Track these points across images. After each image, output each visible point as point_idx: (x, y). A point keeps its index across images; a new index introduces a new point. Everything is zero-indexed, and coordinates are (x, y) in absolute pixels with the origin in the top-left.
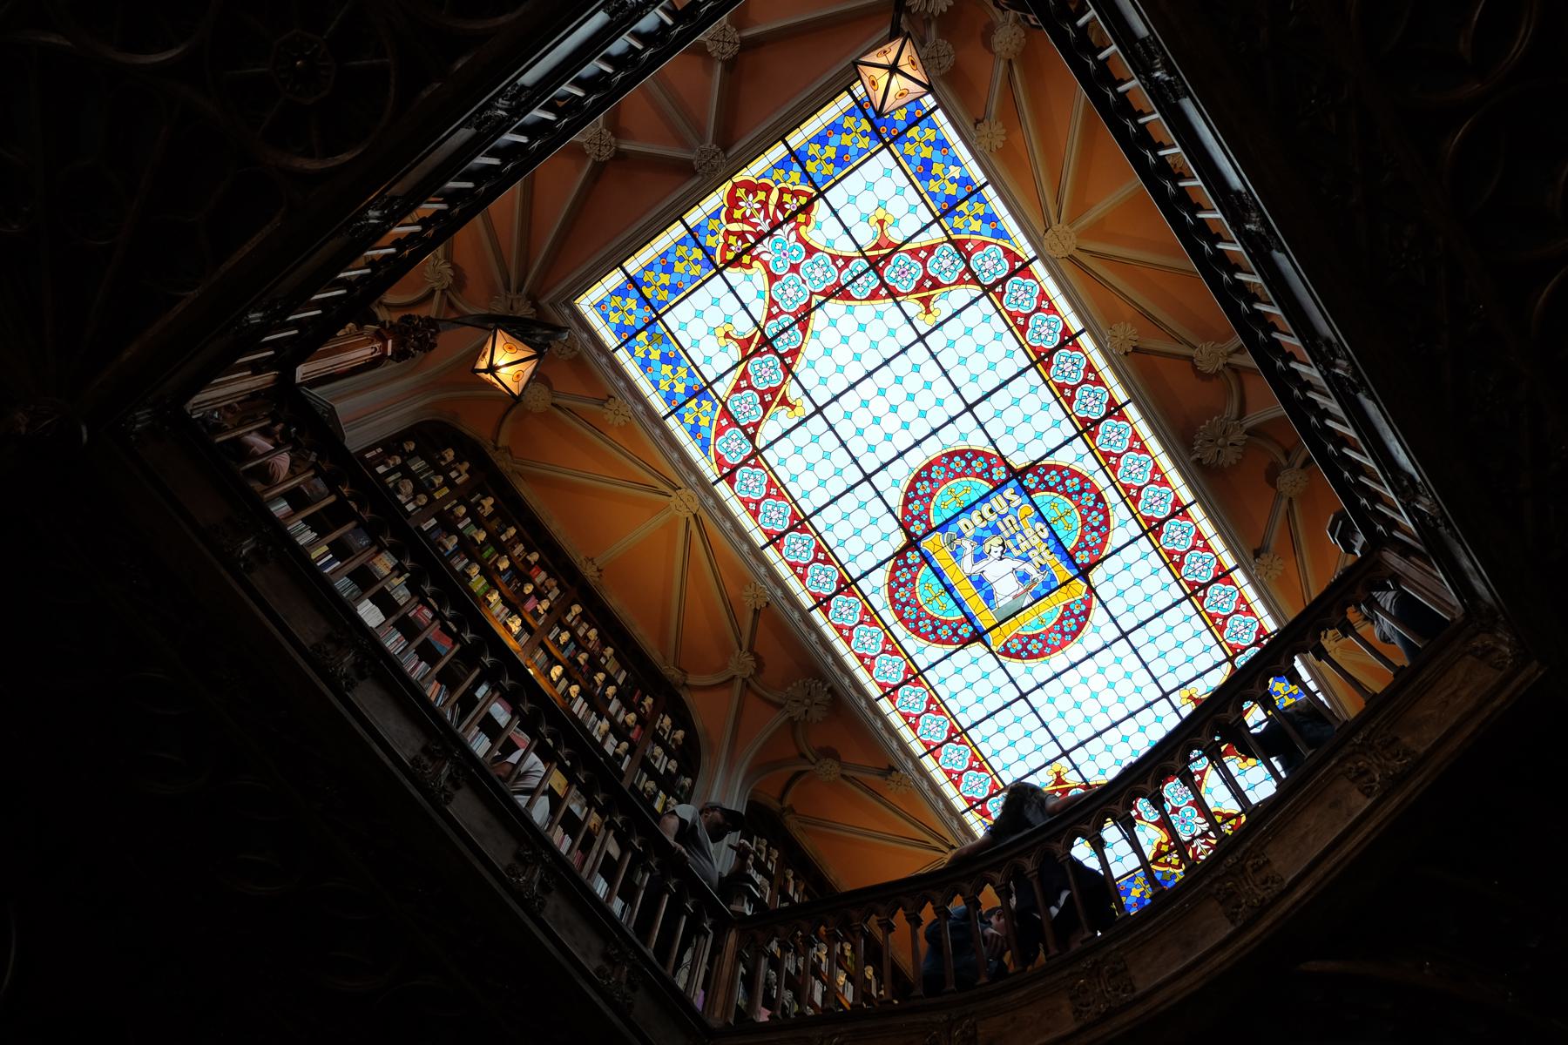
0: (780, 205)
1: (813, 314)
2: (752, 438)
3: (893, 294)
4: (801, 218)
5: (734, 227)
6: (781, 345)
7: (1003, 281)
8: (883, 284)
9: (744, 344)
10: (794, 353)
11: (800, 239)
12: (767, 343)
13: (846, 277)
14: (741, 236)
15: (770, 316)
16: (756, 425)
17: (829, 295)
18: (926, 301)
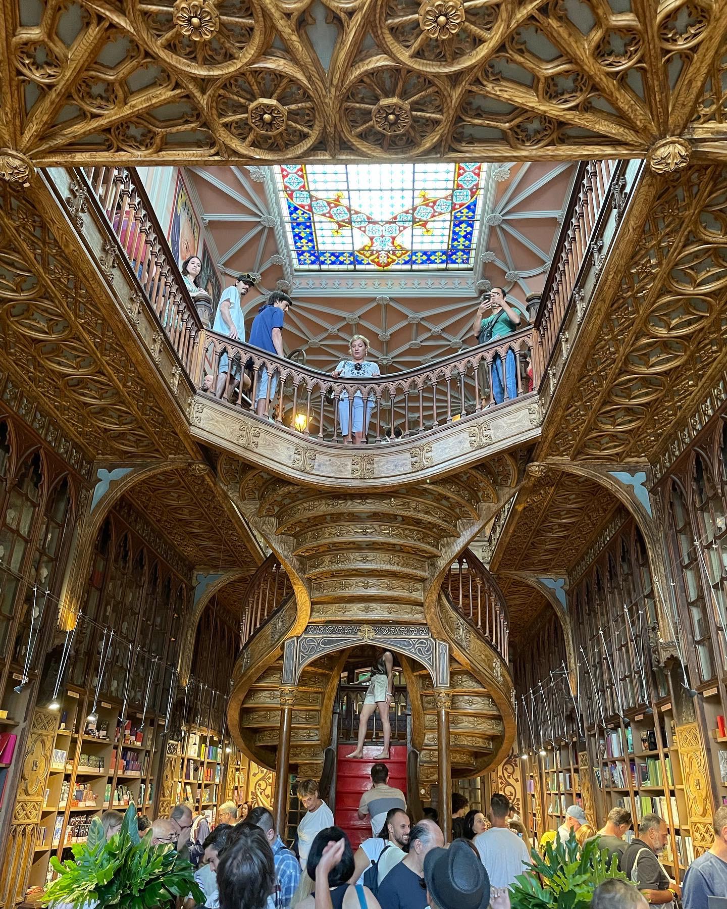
0: (372, 254)
1: (387, 220)
2: (452, 196)
3: (349, 210)
4: (367, 248)
5: (394, 257)
6: (410, 217)
7: (299, 190)
8: (351, 215)
9: (424, 225)
10: (407, 212)
11: (372, 243)
12: (414, 221)
13: (363, 224)
14: (394, 254)
15: (405, 228)
16: (446, 198)
17: (376, 223)
18: (337, 200)
